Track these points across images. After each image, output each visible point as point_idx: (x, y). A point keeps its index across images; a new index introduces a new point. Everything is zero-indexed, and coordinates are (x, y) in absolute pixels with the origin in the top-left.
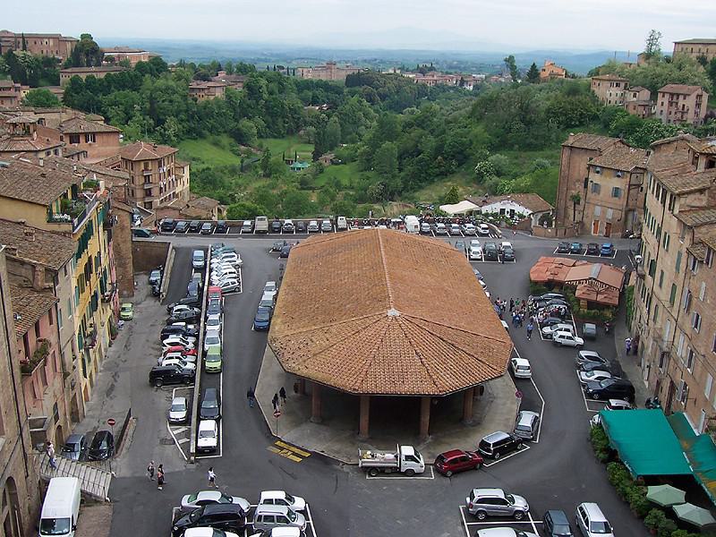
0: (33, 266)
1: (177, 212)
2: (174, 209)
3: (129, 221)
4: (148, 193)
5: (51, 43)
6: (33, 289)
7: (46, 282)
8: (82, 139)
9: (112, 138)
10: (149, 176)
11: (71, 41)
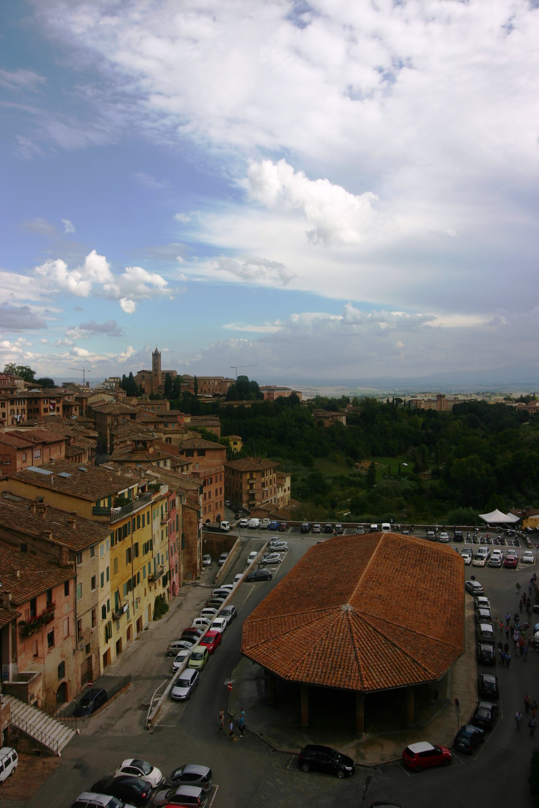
0: (61, 547)
1: (267, 513)
2: (265, 511)
3: (196, 517)
4: (252, 497)
5: (216, 384)
6: (58, 565)
7: (70, 560)
8: (195, 454)
9: (218, 454)
10: (253, 484)
11: (231, 381)
